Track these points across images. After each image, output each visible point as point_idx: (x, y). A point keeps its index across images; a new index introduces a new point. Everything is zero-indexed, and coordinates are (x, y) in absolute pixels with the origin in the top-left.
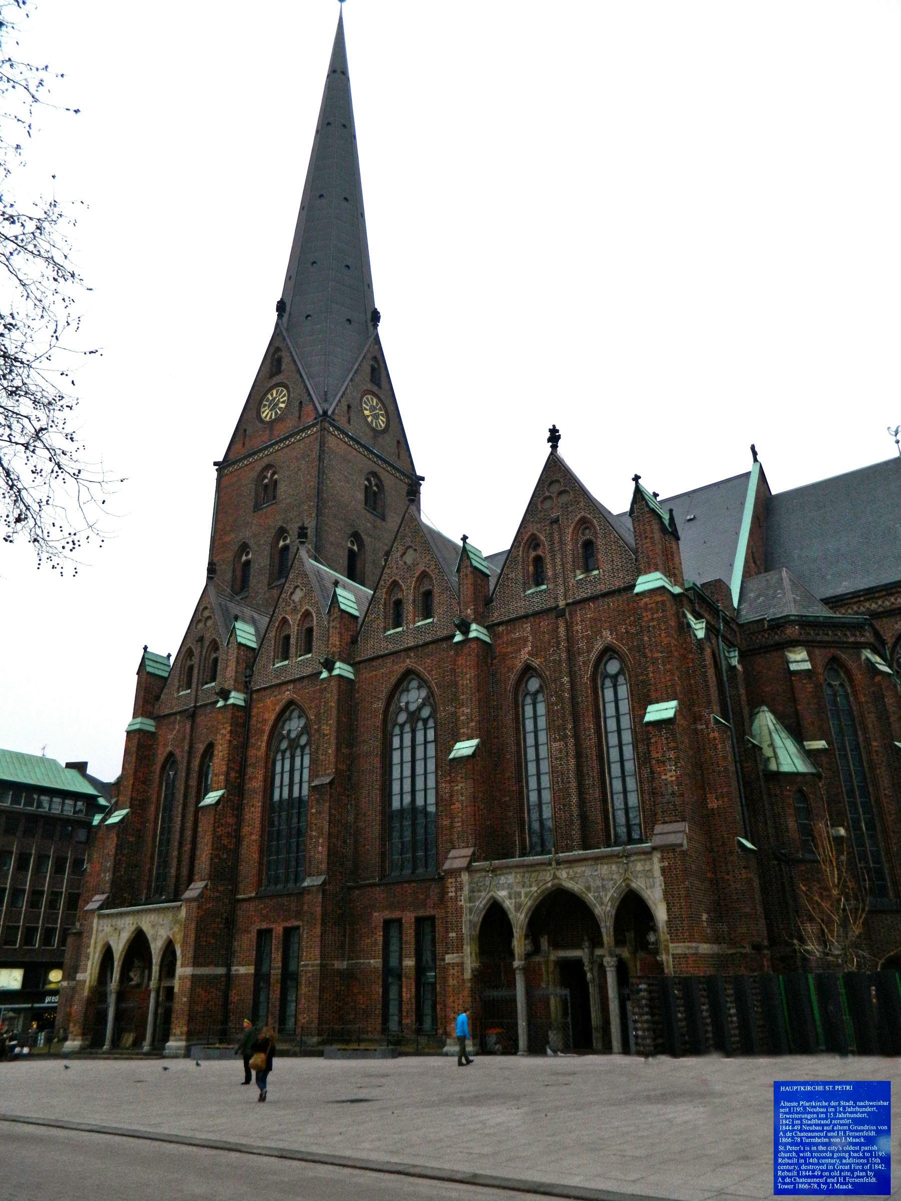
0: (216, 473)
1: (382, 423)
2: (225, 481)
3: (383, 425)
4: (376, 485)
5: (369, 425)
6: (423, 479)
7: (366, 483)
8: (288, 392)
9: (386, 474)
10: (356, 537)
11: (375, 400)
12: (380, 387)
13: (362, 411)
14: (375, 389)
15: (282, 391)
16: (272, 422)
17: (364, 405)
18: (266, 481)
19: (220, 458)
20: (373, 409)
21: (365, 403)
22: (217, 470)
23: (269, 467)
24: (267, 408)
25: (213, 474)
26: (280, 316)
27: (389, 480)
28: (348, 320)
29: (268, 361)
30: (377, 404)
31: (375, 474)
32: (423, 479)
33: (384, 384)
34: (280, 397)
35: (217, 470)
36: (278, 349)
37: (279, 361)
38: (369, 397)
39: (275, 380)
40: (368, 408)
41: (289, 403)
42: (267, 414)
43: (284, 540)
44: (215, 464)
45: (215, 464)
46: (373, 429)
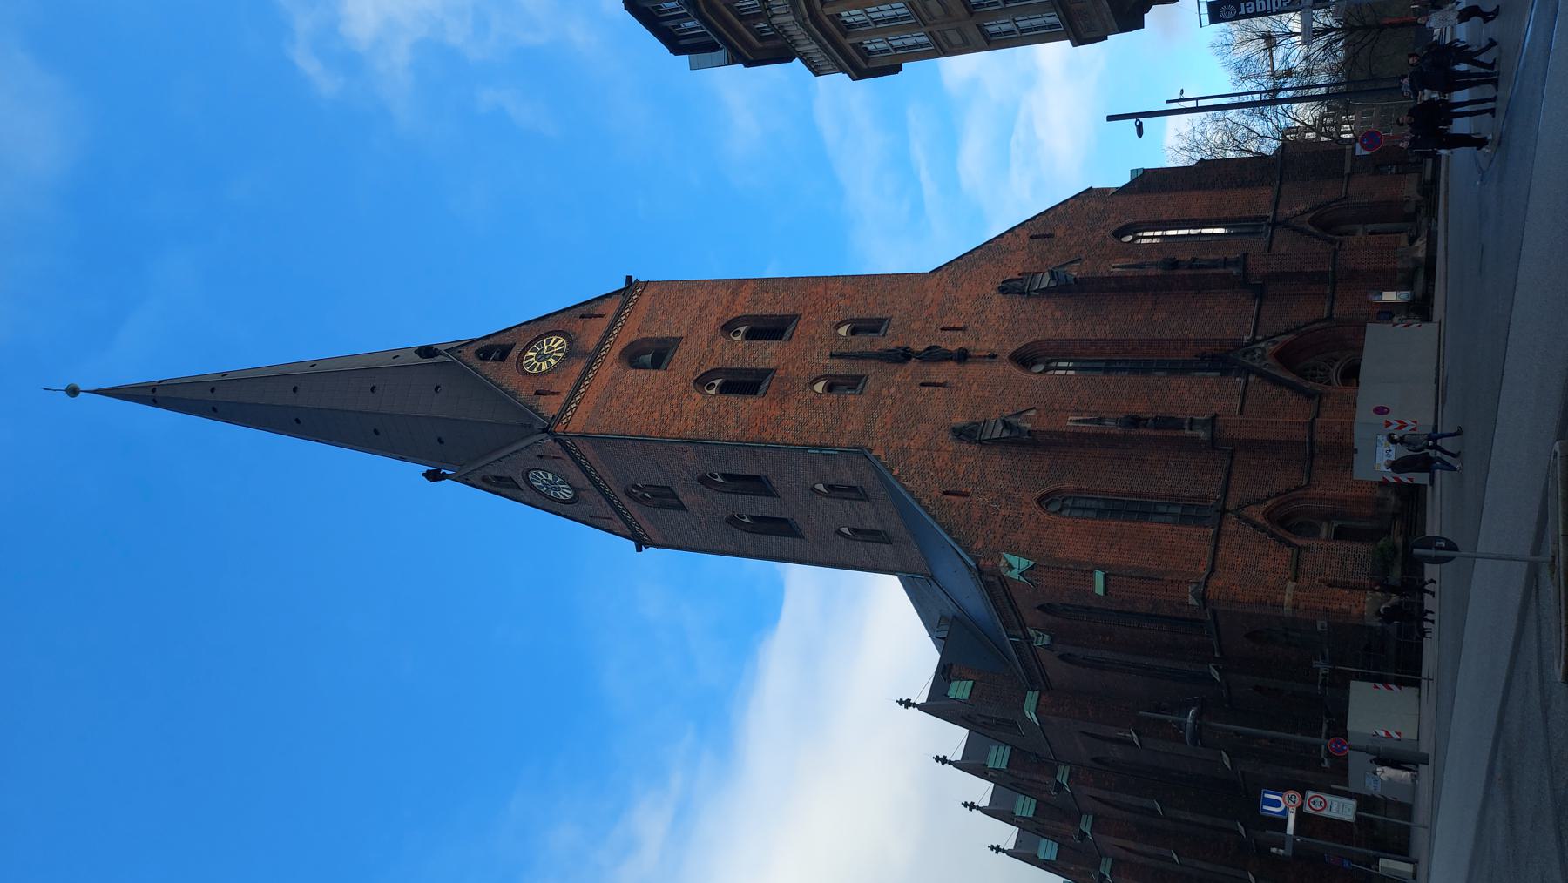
0: (651, 549)
1: (557, 343)
2: (658, 539)
3: (560, 341)
5: (562, 363)
6: (629, 278)
8: (534, 469)
10: (703, 381)
11: (529, 354)
12: (512, 346)
13: (541, 374)
14: (514, 354)
15: (532, 476)
16: (572, 487)
18: (647, 495)
19: (632, 544)
20: (542, 357)
21: (532, 369)
22: (646, 548)
23: (628, 494)
25: (650, 552)
26: (444, 477)
27: (630, 333)
28: (436, 389)
29: (503, 491)
30: (535, 350)
32: (629, 278)
33: (506, 339)
34: (542, 478)
35: (646, 548)
36: (484, 479)
37: (498, 478)
38: (525, 362)
39: (522, 485)
40: (539, 364)
41: (546, 472)
42: (566, 493)
43: (716, 477)
44: (639, 550)
45: (639, 550)
46: (566, 356)
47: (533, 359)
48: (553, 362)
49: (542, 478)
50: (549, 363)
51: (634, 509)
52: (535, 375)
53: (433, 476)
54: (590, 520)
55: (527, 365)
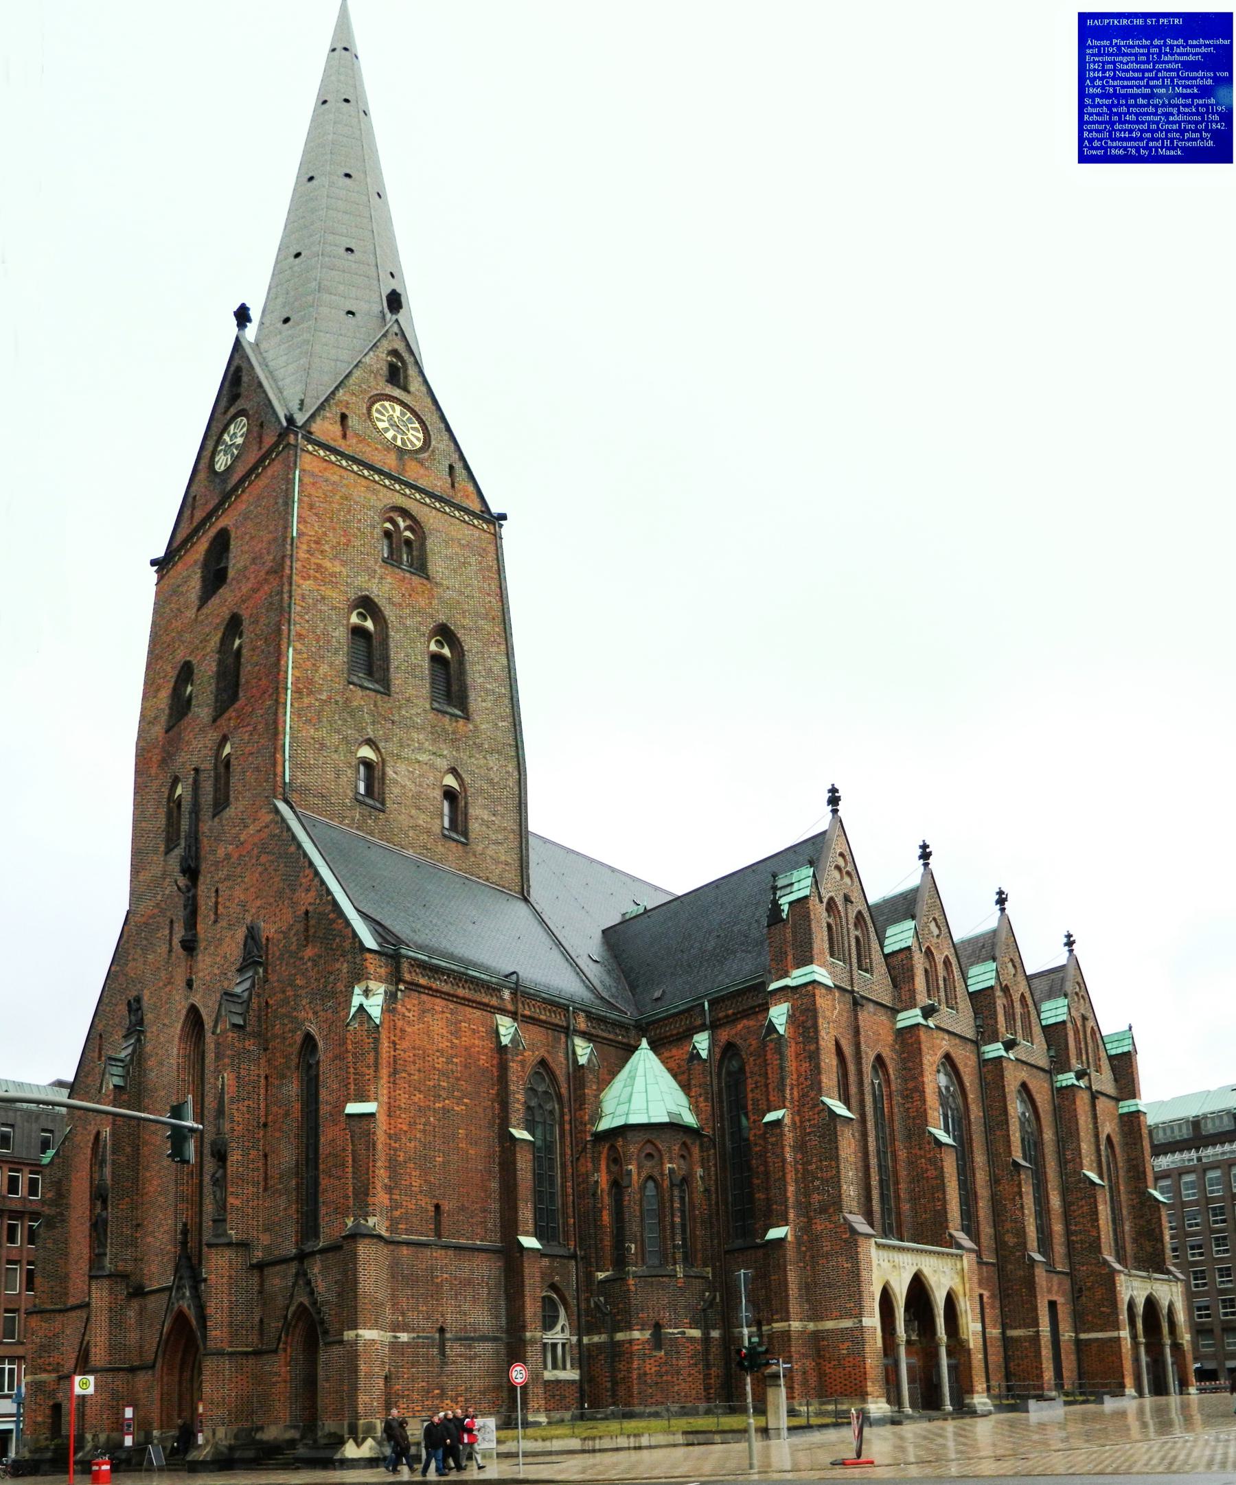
1: (415, 438)
4: (408, 528)
5: (391, 447)
7: (388, 525)
9: (426, 509)
11: (398, 408)
14: (397, 393)
16: (229, 469)
17: (375, 415)
21: (378, 411)
24: (222, 454)
30: (403, 414)
31: (405, 513)
36: (239, 370)
38: (387, 404)
39: (232, 411)
40: (385, 419)
42: (222, 462)
47: (387, 415)
48: (389, 435)
49: (237, 434)
50: (386, 430)
51: (202, 546)
52: (369, 409)
53: (242, 316)
54: (190, 499)
55: (383, 406)
